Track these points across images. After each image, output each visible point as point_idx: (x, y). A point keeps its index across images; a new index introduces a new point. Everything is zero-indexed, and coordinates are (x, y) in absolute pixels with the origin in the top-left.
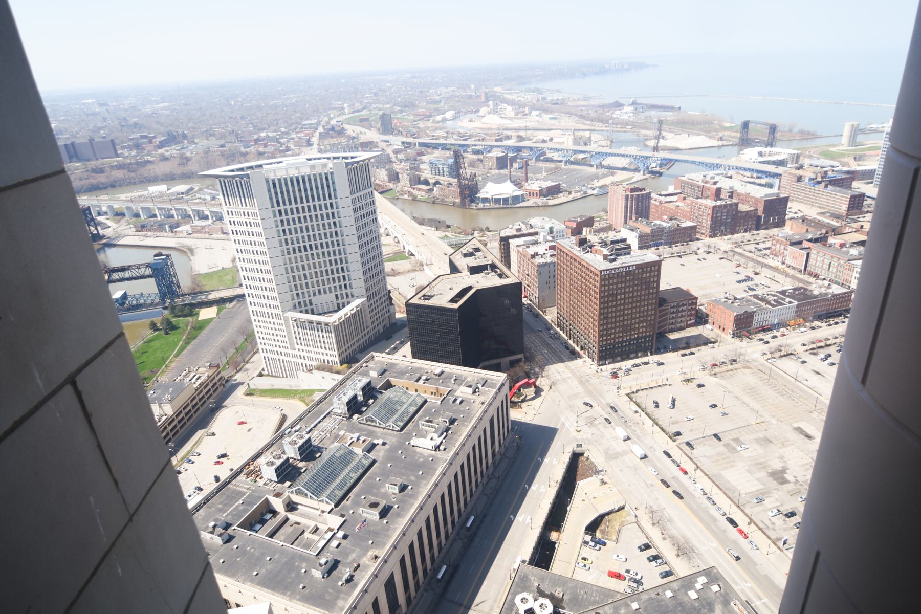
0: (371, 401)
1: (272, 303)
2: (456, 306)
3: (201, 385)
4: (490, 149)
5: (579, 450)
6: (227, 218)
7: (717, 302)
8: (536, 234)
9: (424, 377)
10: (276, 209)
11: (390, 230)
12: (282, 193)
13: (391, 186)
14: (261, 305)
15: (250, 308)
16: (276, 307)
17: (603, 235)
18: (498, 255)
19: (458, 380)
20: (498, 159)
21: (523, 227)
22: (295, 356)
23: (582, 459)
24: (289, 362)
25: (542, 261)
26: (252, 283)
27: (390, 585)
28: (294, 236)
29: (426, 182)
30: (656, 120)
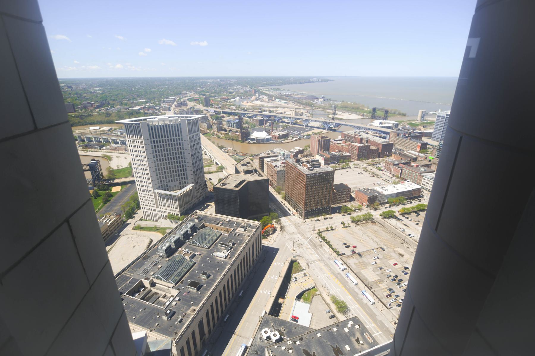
0: (195, 234)
2: (237, 189)
4: (256, 116)
5: (294, 259)
6: (128, 144)
7: (360, 191)
8: (276, 156)
9: (221, 223)
10: (152, 140)
11: (207, 152)
12: (155, 133)
13: (208, 131)
14: (142, 186)
15: (137, 187)
16: (150, 187)
17: (309, 159)
18: (258, 166)
19: (238, 225)
20: (259, 120)
21: (271, 153)
22: (158, 211)
23: (294, 263)
24: (155, 214)
25: (279, 169)
26: (139, 175)
27: (201, 324)
29: (225, 130)
30: (333, 106)
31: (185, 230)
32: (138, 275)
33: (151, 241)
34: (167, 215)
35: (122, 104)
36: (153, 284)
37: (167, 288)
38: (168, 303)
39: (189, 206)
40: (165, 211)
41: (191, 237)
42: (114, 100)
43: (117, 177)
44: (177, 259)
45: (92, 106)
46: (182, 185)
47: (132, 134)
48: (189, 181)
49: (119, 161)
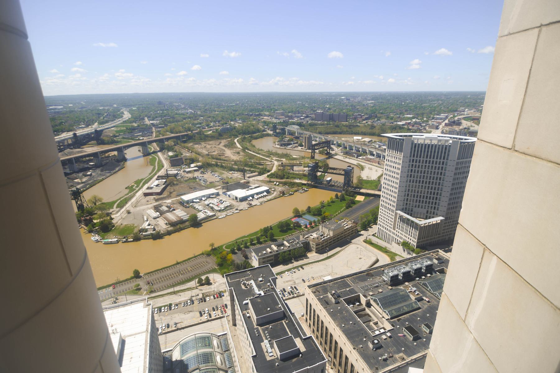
1: (392, 203)
3: (347, 228)
14: (386, 203)
16: (393, 206)
22: (394, 233)
24: (389, 235)
26: (386, 191)
28: (416, 174)
31: (419, 266)
32: (358, 287)
33: (377, 261)
34: (402, 241)
35: (388, 117)
36: (369, 305)
37: (381, 316)
38: (377, 333)
39: (429, 241)
40: (401, 236)
41: (423, 277)
42: (382, 113)
43: (364, 187)
44: (401, 293)
45: (361, 117)
46: (429, 215)
47: (393, 149)
48: (439, 213)
49: (370, 172)
